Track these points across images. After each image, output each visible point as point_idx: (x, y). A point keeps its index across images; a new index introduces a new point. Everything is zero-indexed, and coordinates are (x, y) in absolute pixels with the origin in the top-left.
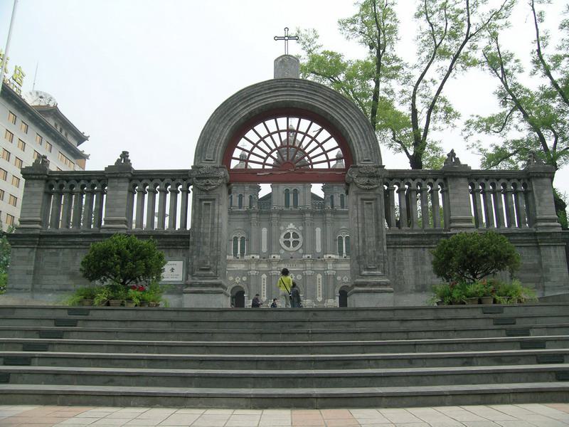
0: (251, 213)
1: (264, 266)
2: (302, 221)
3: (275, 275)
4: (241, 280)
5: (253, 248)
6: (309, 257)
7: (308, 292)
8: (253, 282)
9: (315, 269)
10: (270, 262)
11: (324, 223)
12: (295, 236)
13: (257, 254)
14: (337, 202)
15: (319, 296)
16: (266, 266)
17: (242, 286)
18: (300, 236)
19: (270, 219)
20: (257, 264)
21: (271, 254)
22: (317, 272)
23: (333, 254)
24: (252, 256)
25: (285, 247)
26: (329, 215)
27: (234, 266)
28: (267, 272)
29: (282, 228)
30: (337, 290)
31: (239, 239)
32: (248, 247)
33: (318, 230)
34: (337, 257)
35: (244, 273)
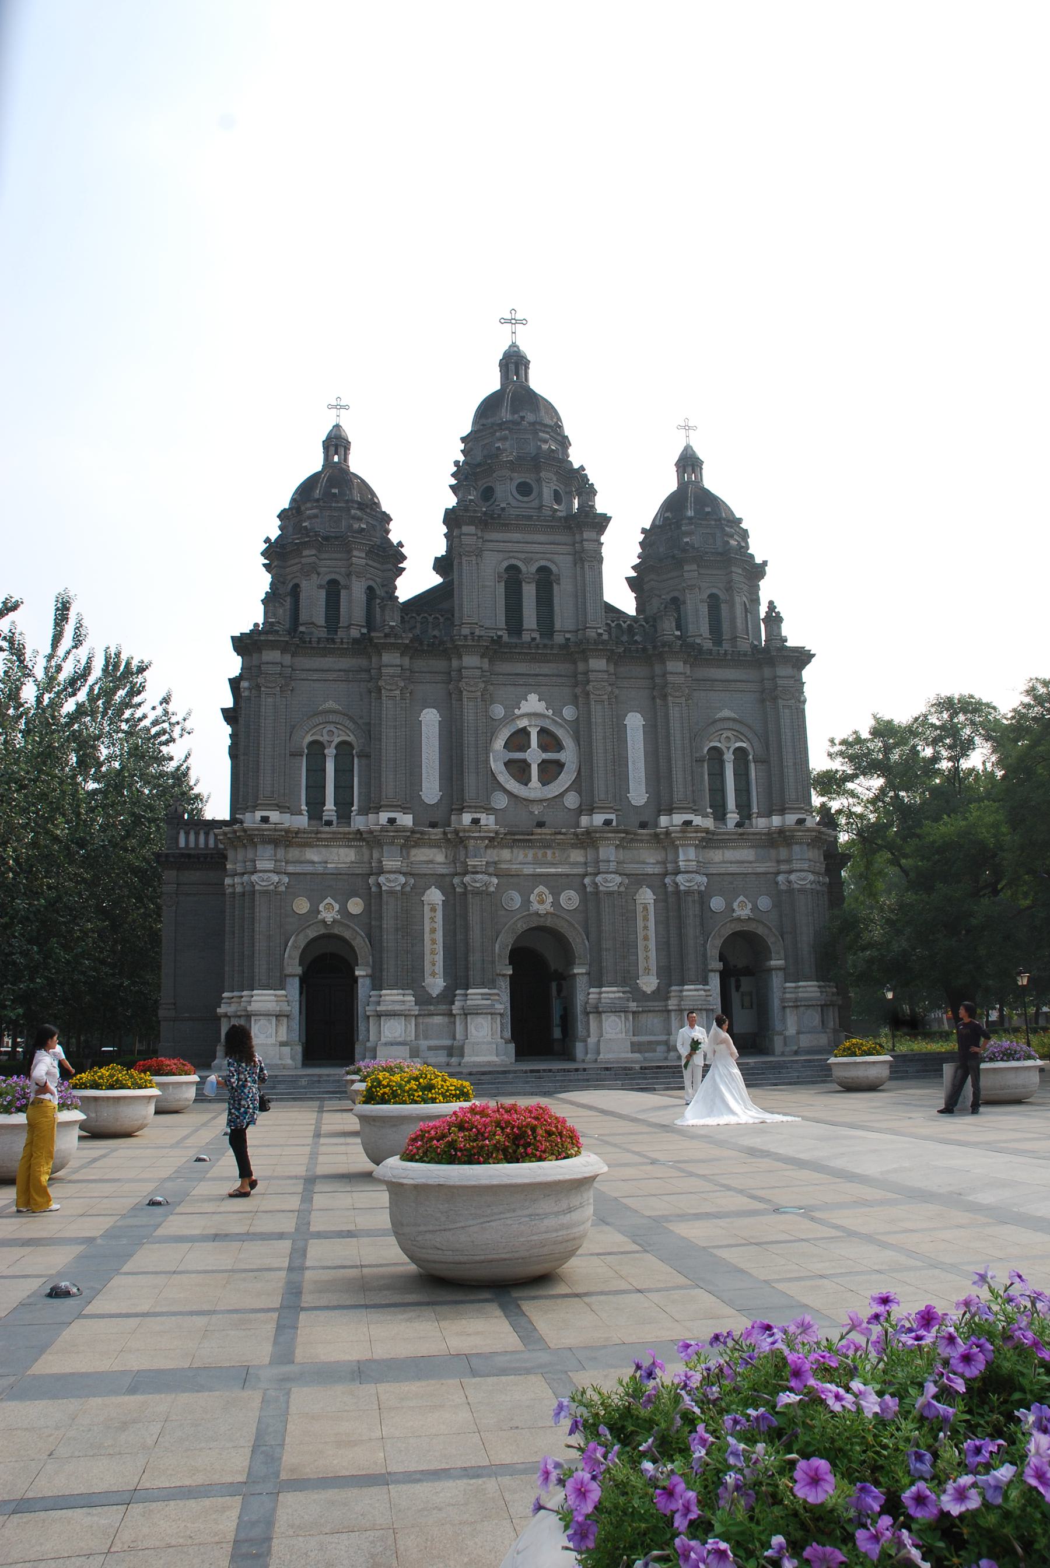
0: (379, 649)
3: (477, 893)
4: (344, 911)
5: (390, 785)
6: (608, 822)
9: (631, 868)
10: (457, 842)
12: (549, 741)
13: (405, 810)
15: (647, 970)
16: (439, 856)
17: (347, 934)
18: (568, 742)
21: (461, 810)
22: (638, 880)
23: (695, 811)
24: (384, 817)
25: (512, 785)
26: (675, 666)
31: (330, 752)
32: (366, 784)
34: (709, 823)
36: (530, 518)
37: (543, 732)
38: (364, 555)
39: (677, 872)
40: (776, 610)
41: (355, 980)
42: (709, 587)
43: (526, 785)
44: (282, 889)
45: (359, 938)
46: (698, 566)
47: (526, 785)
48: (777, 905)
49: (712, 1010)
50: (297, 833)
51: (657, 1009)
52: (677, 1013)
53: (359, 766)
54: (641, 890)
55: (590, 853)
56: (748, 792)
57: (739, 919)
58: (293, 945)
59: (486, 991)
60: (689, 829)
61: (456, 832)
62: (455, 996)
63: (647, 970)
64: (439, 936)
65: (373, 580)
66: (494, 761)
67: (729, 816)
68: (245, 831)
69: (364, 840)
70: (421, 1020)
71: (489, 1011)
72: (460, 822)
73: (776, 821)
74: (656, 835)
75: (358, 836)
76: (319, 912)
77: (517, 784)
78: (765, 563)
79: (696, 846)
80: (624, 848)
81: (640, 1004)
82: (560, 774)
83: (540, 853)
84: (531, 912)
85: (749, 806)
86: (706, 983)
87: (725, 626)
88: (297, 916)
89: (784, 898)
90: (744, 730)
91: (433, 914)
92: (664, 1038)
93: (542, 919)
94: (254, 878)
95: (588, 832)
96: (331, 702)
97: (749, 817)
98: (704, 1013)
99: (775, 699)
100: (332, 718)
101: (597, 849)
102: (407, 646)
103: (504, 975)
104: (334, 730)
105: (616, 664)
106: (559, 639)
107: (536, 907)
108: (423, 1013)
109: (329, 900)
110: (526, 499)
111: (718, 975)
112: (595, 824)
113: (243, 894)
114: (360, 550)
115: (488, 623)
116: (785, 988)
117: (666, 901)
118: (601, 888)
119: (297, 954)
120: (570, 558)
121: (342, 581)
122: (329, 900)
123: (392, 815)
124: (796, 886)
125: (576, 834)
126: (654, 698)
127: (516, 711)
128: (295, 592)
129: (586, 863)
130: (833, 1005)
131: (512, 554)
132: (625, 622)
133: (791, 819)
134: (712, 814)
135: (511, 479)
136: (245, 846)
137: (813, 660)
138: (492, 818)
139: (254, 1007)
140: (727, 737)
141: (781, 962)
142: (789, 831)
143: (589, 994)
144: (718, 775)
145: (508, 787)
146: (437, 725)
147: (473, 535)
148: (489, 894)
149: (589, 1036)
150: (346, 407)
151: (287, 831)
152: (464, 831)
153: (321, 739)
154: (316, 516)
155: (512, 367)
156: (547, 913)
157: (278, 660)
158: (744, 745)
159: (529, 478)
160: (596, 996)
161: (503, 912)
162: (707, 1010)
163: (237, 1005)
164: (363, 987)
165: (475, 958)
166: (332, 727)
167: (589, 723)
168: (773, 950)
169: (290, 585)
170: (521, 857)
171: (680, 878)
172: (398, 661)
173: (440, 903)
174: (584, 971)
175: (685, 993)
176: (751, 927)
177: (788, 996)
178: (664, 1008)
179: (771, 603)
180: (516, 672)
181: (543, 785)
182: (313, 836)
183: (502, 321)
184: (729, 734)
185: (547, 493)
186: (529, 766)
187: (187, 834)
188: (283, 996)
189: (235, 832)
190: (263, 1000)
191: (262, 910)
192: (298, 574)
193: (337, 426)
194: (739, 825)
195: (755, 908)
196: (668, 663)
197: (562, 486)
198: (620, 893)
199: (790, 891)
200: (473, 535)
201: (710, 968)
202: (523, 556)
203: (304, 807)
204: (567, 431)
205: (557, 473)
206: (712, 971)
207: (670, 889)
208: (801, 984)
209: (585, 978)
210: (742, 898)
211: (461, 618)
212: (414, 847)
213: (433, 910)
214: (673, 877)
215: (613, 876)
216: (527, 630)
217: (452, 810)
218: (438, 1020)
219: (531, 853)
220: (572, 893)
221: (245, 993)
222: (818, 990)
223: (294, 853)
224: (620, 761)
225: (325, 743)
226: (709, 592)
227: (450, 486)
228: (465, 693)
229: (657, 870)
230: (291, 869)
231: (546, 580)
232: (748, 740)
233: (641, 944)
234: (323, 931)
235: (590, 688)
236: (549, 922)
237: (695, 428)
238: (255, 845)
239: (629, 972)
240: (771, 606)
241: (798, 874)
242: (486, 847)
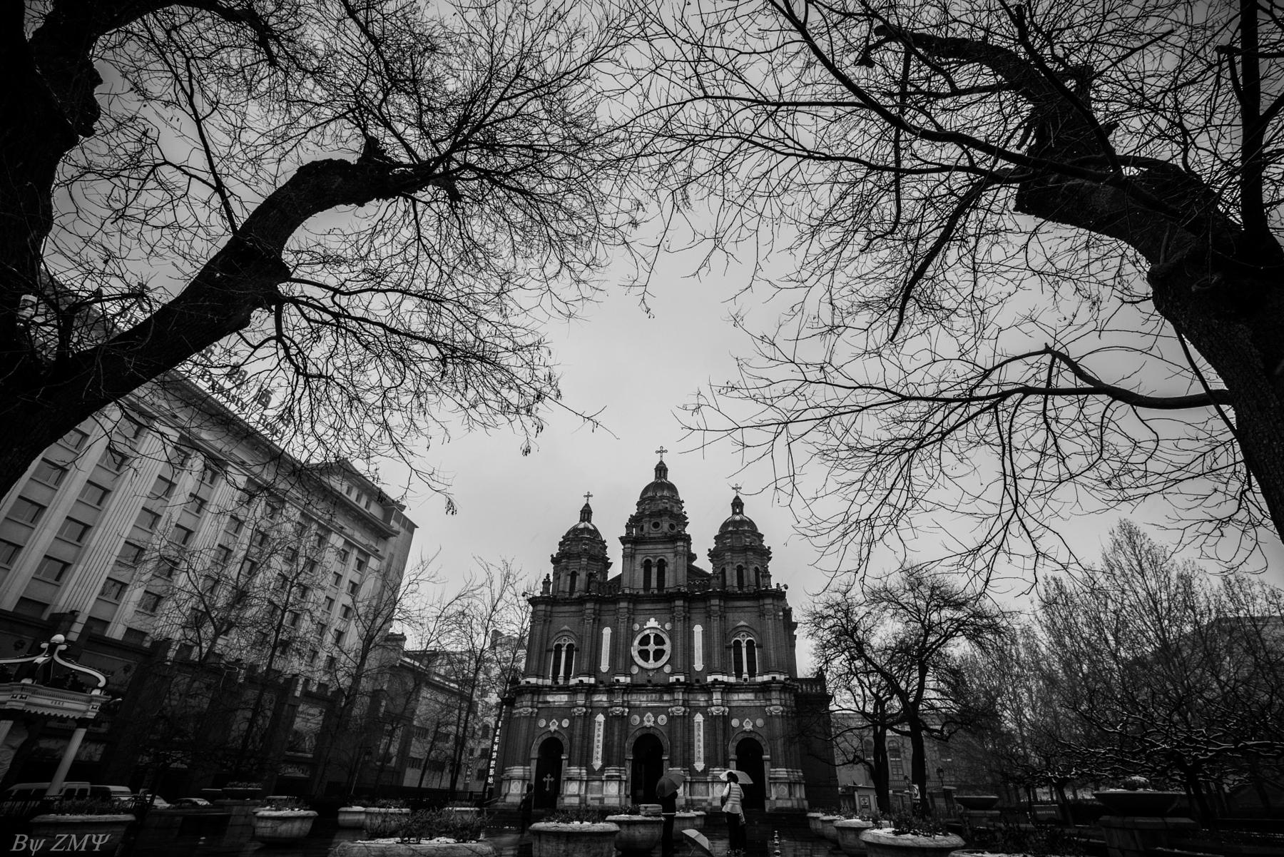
1: (601, 698)
2: (671, 610)
3: (617, 716)
4: (560, 726)
6: (678, 680)
7: (678, 751)
10: (611, 689)
12: (659, 640)
13: (590, 676)
14: (732, 580)
16: (604, 698)
17: (560, 738)
18: (667, 641)
19: (616, 612)
20: (587, 694)
21: (614, 675)
23: (723, 674)
27: (549, 698)
28: (605, 710)
29: (637, 627)
30: (732, 748)
31: (564, 649)
33: (698, 629)
37: (657, 636)
39: (713, 705)
57: (745, 731)
64: (601, 738)
87: (745, 579)
89: (769, 719)
92: (705, 798)
119: (537, 747)
130: (800, 783)
171: (713, 709)
176: (753, 735)
190: (518, 771)
191: (524, 726)
195: (754, 725)
199: (771, 716)
209: (668, 762)
218: (597, 783)
220: (664, 716)
230: (540, 705)
231: (662, 565)
236: (652, 731)
242: (623, 694)
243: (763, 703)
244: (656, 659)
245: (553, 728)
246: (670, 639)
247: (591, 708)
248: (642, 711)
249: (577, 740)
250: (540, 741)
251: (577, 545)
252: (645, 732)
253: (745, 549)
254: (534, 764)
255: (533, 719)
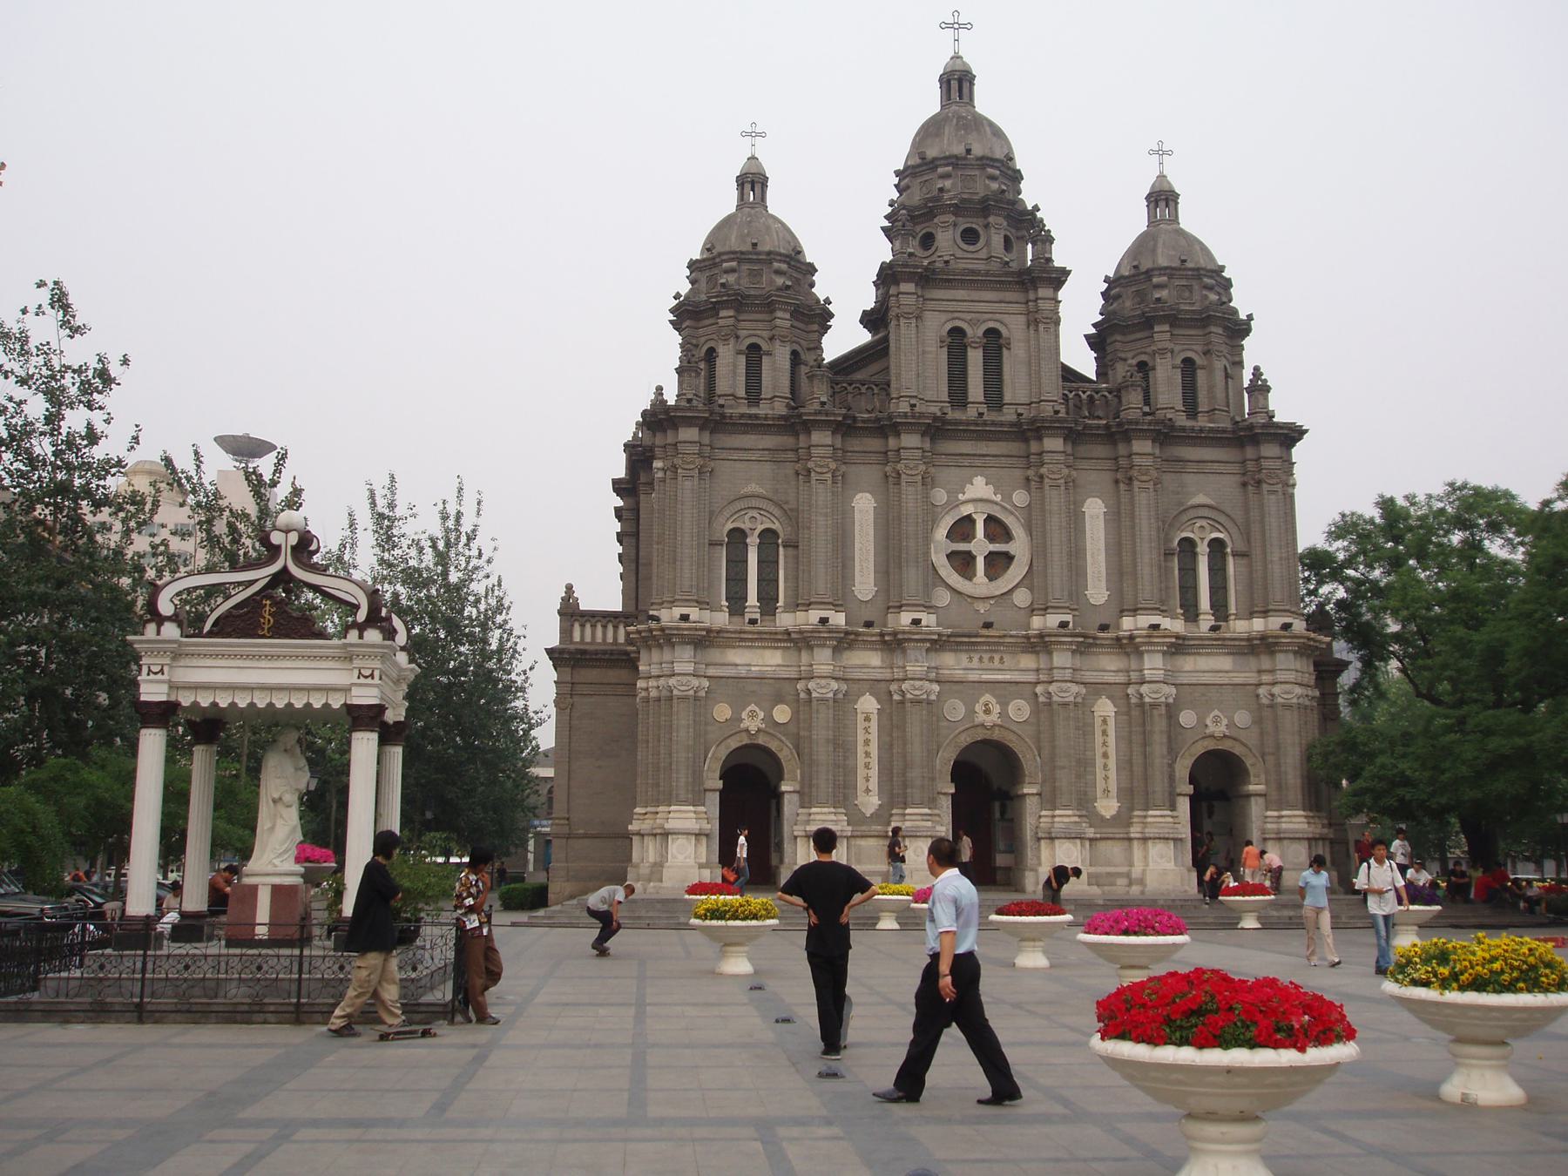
0: (807, 427)
1: (869, 660)
2: (1031, 461)
3: (917, 702)
4: (769, 718)
6: (1064, 625)
7: (1064, 779)
8: (821, 732)
9: (1090, 676)
10: (894, 644)
11: (1123, 477)
12: (996, 528)
13: (836, 607)
17: (773, 746)
18: (1018, 531)
20: (837, 650)
23: (1163, 612)
24: (814, 616)
25: (954, 579)
26: (1142, 446)
28: (877, 687)
29: (940, 496)
30: (1183, 768)
31: (753, 541)
33: (1095, 509)
34: (1174, 625)
35: (776, 689)
36: (973, 272)
37: (990, 520)
38: (788, 316)
40: (1263, 377)
41: (778, 796)
42: (1183, 350)
43: (970, 580)
44: (702, 694)
45: (785, 748)
46: (1171, 326)
47: (970, 580)
48: (1258, 721)
49: (1181, 840)
50: (718, 632)
51: (1117, 836)
52: (1141, 841)
53: (785, 557)
54: (1100, 701)
55: (1043, 658)
56: (1225, 588)
57: (1212, 736)
58: (713, 755)
59: (926, 811)
60: (1155, 633)
61: (895, 634)
62: (892, 815)
63: (1106, 791)
64: (874, 749)
65: (797, 343)
66: (935, 553)
67: (1201, 617)
68: (662, 629)
69: (791, 640)
70: (853, 842)
71: (929, 833)
72: (898, 620)
73: (1258, 625)
74: (1118, 639)
75: (785, 637)
76: (742, 720)
77: (960, 579)
78: (1250, 317)
79: (1164, 653)
80: (1082, 653)
81: (1099, 830)
82: (1008, 568)
83: (986, 656)
84: (976, 723)
85: (1226, 606)
86: (1173, 807)
88: (717, 724)
89: (1266, 713)
90: (1222, 519)
91: (867, 724)
92: (1124, 869)
93: (989, 732)
94: (672, 681)
95: (1041, 636)
96: (753, 485)
97: (1226, 618)
98: (1171, 844)
99: (1259, 482)
100: (754, 502)
101: (1050, 653)
102: (839, 424)
103: (945, 794)
104: (757, 516)
105: (1074, 443)
106: (1009, 415)
107: (981, 717)
108: (855, 833)
109: (753, 707)
110: (971, 248)
111: (1187, 800)
112: (1048, 625)
113: (659, 699)
114: (785, 310)
115: (929, 395)
116: (1266, 817)
117: (1128, 713)
118: (1055, 698)
120: (1022, 319)
121: (765, 347)
122: (753, 707)
123: (824, 614)
124: (1279, 700)
125: (1027, 637)
126: (1117, 482)
127: (960, 496)
128: (711, 355)
129: (1038, 670)
130: (1323, 839)
131: (956, 315)
132: (1084, 392)
133: (1275, 623)
134: (1182, 615)
135: (955, 225)
136: (660, 647)
137: (1305, 436)
138: (933, 618)
139: (671, 825)
140: (1202, 527)
141: (1261, 787)
142: (1272, 637)
143: (1040, 817)
144: (1189, 571)
145: (950, 582)
146: (872, 512)
147: (913, 294)
148: (929, 703)
149: (1040, 864)
150: (762, 135)
151: (709, 631)
152: (904, 632)
153: (742, 526)
154: (733, 270)
155: (954, 84)
156: (994, 725)
157: (696, 439)
158: (1221, 535)
159: (976, 224)
160: (1049, 820)
161: (946, 724)
162: (1175, 840)
163: (651, 822)
164: (790, 805)
165: (915, 774)
166: (754, 513)
167: (1043, 510)
168: (1252, 774)
169: (705, 348)
170: (975, 663)
171: (1144, 689)
172: (829, 441)
173: (876, 712)
174: (1035, 791)
175: (1149, 820)
177: (1269, 826)
178: (1125, 836)
179: (1257, 369)
180: (961, 452)
181: (991, 580)
182: (737, 636)
183: (943, 25)
184: (1204, 523)
185: (997, 240)
186: (974, 558)
187: (583, 626)
188: (702, 812)
189: (651, 631)
190: (683, 817)
191: (683, 719)
192: (714, 336)
193: (753, 158)
194: (1214, 629)
196: (1133, 442)
197: (1013, 231)
198: (1076, 704)
200: (913, 294)
201: (1178, 791)
202: (968, 317)
203: (725, 603)
204: (1020, 164)
205: (1007, 217)
206: (1180, 795)
207: (1134, 700)
208: (1285, 813)
210: (1216, 712)
211: (898, 389)
212: (846, 649)
213: (867, 719)
214: (1136, 686)
215: (1069, 685)
216: (973, 403)
217: (889, 608)
219: (976, 657)
221: (661, 809)
222: (1305, 820)
223: (714, 655)
224: (1076, 554)
225: (748, 531)
226: (1183, 356)
227: (883, 228)
228: (903, 476)
229: (1121, 678)
230: (711, 671)
231: (994, 343)
232: (1226, 529)
233: (1099, 762)
234: (746, 741)
235: (1043, 470)
236: (996, 735)
237: (1169, 153)
238: (673, 645)
239: (1085, 793)
240: (1257, 369)
241: (1283, 686)
242: (928, 650)
243: (1251, 678)
244: (992, 574)
245: (753, 725)
246: (1029, 529)
247: (845, 680)
248: (969, 689)
249: (823, 753)
250: (723, 753)
251: (759, 274)
252: (980, 735)
253: (1203, 320)
254: (713, 803)
255: (700, 702)
